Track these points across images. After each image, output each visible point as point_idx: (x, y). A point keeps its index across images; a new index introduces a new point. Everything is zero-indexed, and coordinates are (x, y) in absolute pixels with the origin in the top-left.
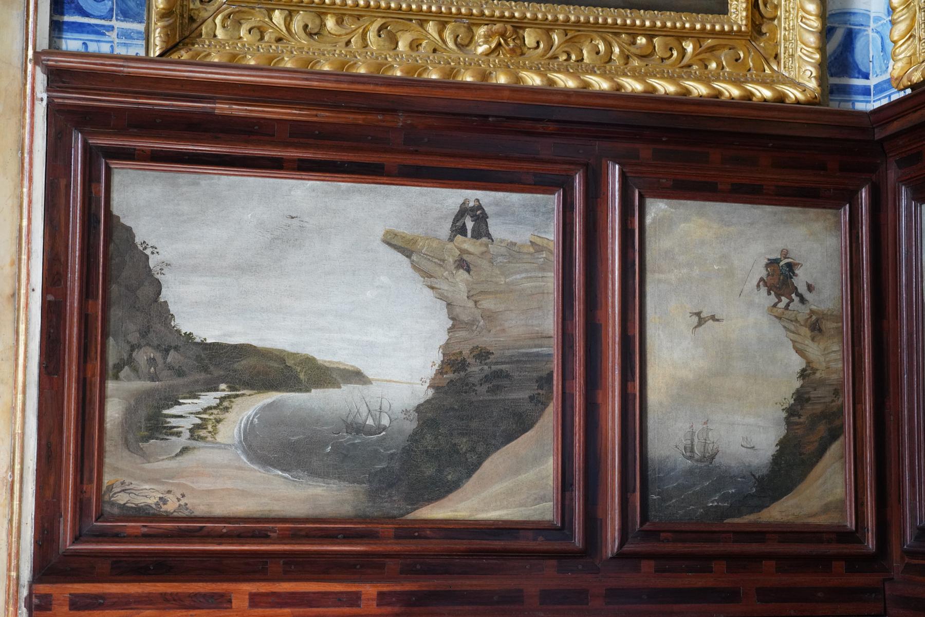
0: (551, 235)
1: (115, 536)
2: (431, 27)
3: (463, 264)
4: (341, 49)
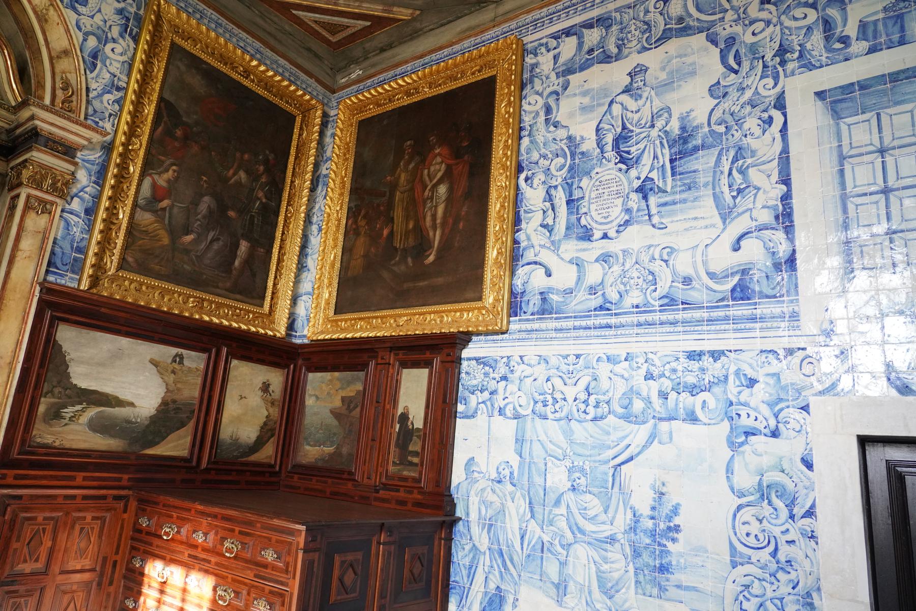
0: (202, 366)
1: (33, 454)
2: (176, 295)
3: (173, 372)
4: (146, 297)
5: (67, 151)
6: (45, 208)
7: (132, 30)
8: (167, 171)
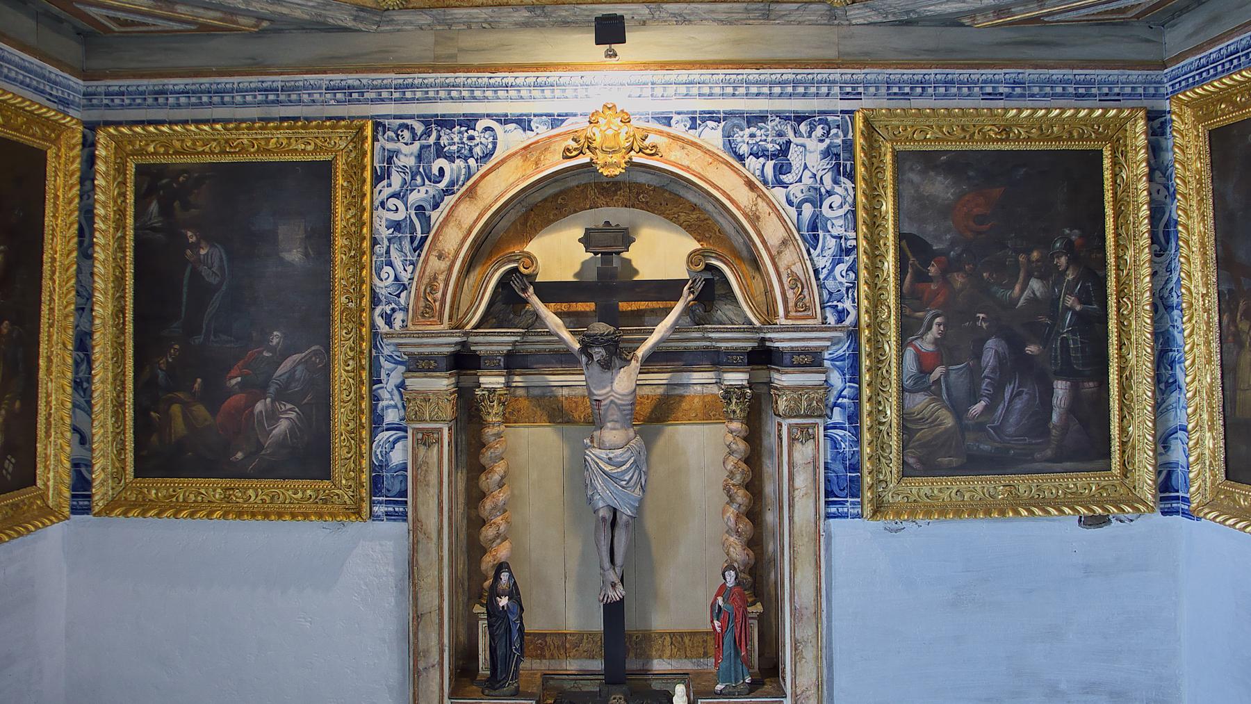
5: (812, 360)
6: (806, 434)
7: (845, 167)
8: (929, 328)
